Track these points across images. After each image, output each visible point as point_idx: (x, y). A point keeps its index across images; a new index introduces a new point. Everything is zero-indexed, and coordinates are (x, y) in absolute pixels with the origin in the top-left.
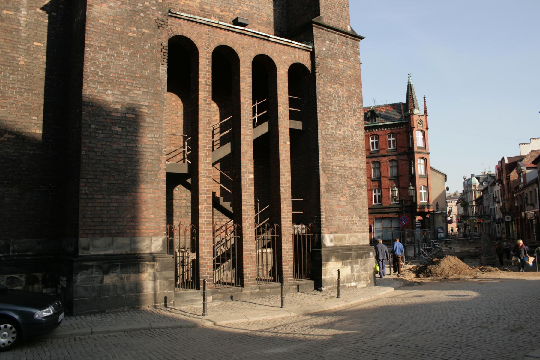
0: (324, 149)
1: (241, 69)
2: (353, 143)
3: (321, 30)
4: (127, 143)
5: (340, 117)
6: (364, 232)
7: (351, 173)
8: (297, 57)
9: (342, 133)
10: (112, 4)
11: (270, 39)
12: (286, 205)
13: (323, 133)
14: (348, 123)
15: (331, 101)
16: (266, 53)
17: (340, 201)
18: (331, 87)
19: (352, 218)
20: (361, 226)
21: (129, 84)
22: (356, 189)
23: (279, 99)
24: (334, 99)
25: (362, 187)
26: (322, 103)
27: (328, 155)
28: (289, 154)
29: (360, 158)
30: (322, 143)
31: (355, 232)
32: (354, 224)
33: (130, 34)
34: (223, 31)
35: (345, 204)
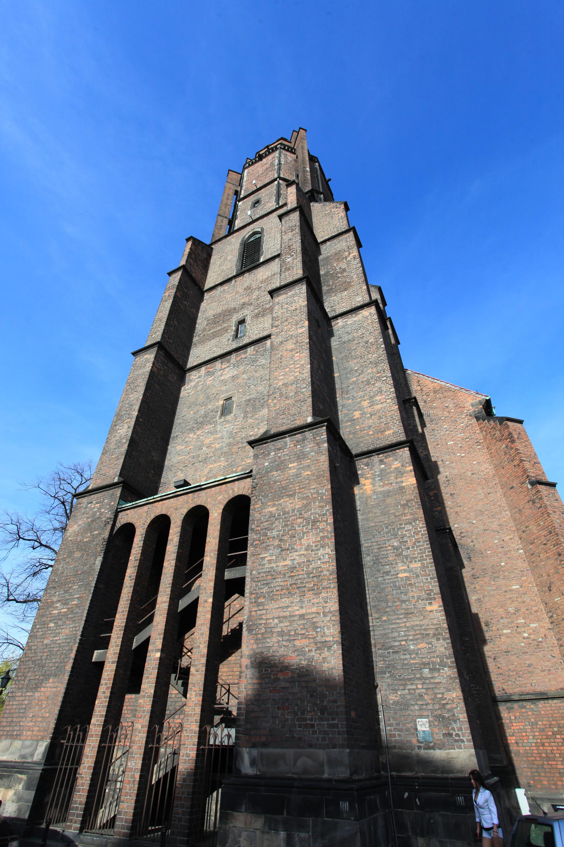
0: (254, 596)
1: (171, 531)
2: (308, 574)
3: (264, 445)
4: (54, 637)
5: (286, 541)
6: (334, 747)
7: (304, 624)
8: (236, 490)
9: (288, 562)
10: (80, 523)
11: (203, 487)
12: (194, 693)
13: (254, 572)
14: (301, 544)
15: (272, 524)
16: (199, 503)
17: (278, 679)
18: (274, 505)
19: (303, 713)
20: (326, 733)
21: (72, 582)
22: (313, 654)
23: (206, 549)
24: (276, 520)
25: (329, 648)
26: (257, 532)
27: (259, 605)
28: (209, 616)
29: (323, 595)
30: (251, 587)
31: (311, 746)
32: (306, 726)
33: (85, 540)
34: (161, 503)
35: (288, 685)
